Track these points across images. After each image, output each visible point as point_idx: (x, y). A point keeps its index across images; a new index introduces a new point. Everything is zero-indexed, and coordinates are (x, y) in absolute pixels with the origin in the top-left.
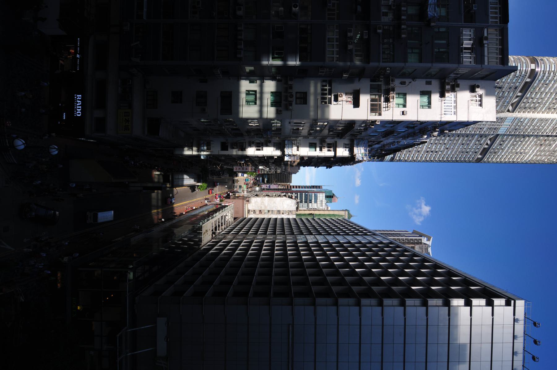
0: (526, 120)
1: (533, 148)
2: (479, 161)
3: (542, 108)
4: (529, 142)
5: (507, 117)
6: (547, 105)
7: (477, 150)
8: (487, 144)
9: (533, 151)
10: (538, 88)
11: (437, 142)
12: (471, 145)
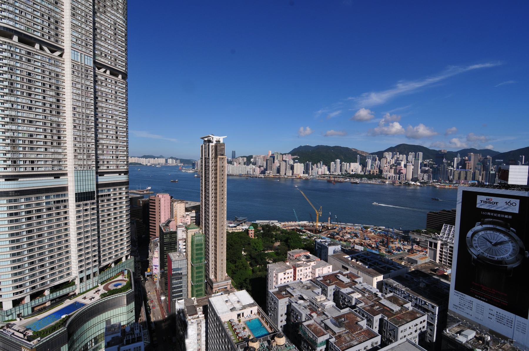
0: (75, 34)
1: (109, 15)
2: (125, 76)
3: (56, 13)
4: (102, 22)
5: (72, 60)
6: (52, 7)
7: (113, 82)
8: (105, 72)
9: (113, 14)
10: (28, 23)
11: (104, 132)
12: (107, 90)
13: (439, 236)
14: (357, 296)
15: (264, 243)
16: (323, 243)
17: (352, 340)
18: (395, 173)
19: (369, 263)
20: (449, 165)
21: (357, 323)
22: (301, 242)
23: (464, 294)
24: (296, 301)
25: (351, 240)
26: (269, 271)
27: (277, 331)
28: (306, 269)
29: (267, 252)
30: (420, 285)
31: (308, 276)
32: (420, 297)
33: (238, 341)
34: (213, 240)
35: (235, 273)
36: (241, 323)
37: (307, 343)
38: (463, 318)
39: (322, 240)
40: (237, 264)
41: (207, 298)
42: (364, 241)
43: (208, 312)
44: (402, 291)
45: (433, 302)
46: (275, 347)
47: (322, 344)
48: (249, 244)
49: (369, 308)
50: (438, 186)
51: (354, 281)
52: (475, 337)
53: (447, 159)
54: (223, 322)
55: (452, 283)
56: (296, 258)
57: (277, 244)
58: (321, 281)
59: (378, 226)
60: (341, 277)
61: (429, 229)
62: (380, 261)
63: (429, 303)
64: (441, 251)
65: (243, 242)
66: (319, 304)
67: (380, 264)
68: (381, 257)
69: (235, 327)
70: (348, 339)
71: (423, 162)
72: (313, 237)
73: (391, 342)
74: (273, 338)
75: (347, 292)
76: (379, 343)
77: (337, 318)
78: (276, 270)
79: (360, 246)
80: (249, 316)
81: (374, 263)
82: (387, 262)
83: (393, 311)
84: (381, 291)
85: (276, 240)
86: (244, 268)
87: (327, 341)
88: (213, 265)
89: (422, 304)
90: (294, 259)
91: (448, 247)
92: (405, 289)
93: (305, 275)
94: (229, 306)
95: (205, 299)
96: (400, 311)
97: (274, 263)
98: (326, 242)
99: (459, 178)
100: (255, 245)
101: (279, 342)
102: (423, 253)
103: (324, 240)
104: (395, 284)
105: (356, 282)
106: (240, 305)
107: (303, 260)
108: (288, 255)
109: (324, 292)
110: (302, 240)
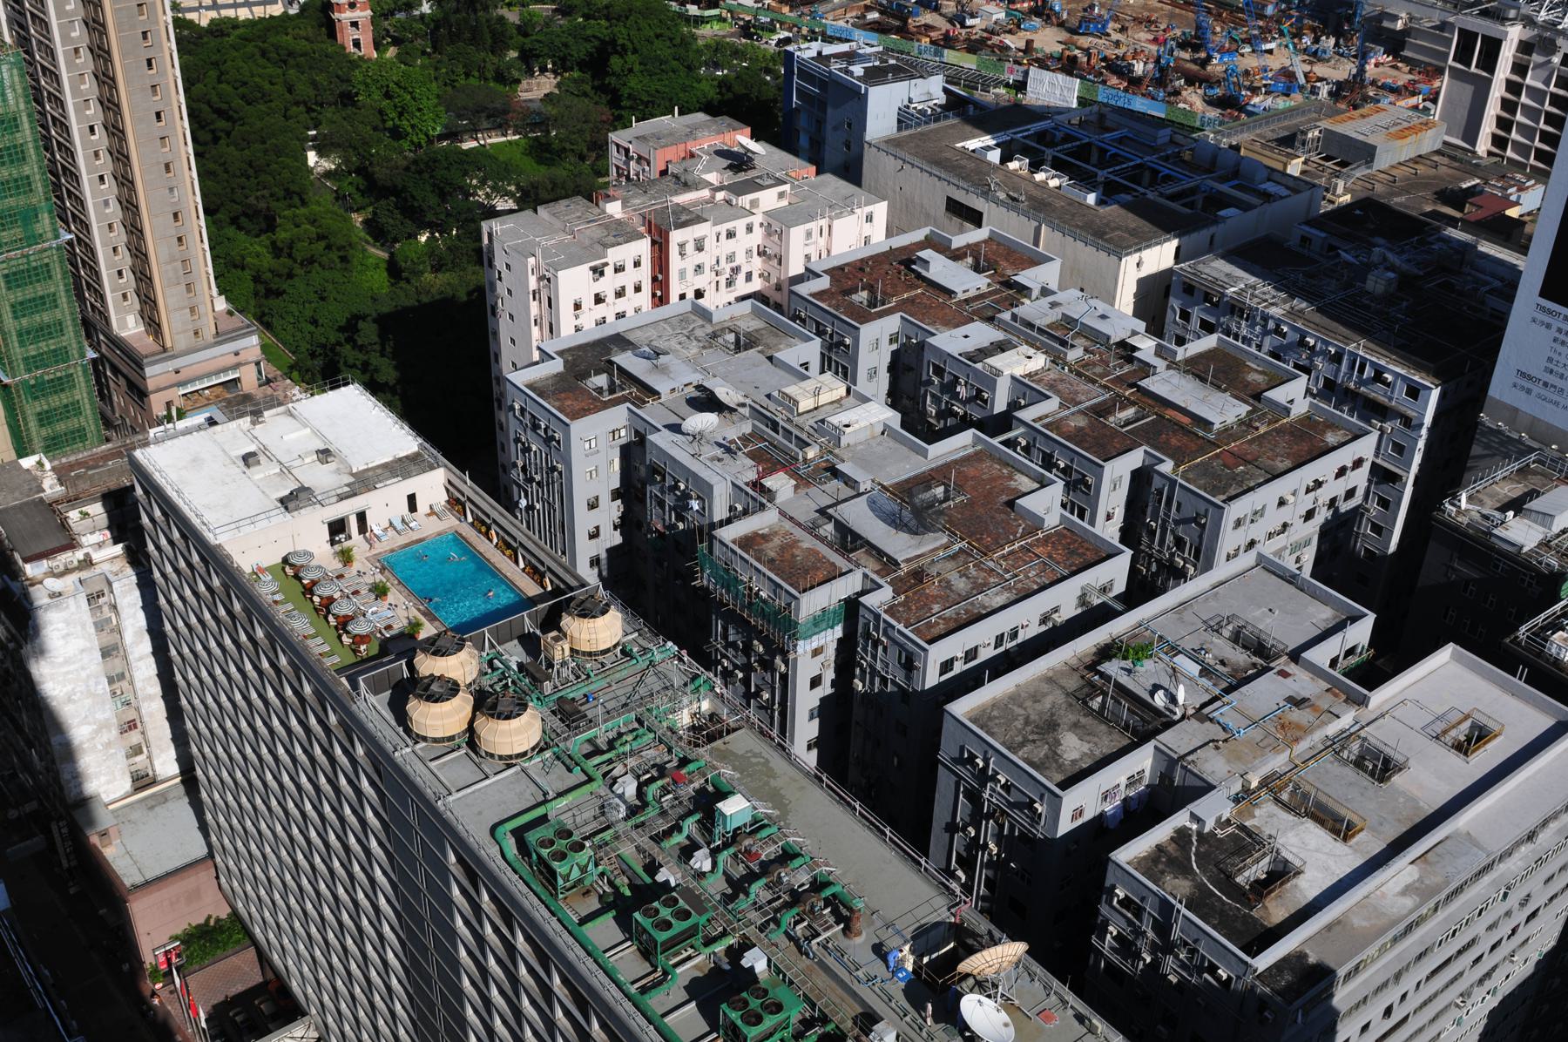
14: (1021, 363)
15: (452, 83)
16: (835, 67)
17: (981, 588)
19: (1102, 175)
21: (1011, 504)
22: (690, 68)
24: (674, 420)
25: (1009, 40)
26: (499, 263)
27: (574, 583)
28: (731, 235)
29: (474, 144)
30: (1370, 284)
31: (741, 277)
32: (1359, 348)
33: (351, 659)
34: (89, 86)
35: (279, 293)
36: (357, 566)
37: (742, 624)
39: (829, 49)
40: (282, 235)
41: (119, 454)
43: (141, 528)
44: (1266, 318)
45: (1419, 368)
46: (564, 664)
47: (821, 621)
48: (348, 99)
49: (1081, 422)
51: (1008, 284)
54: (248, 570)
56: (664, 173)
57: (538, 87)
58: (820, 295)
60: (939, 268)
62: (1166, 159)
63: (1397, 375)
64: (1513, 87)
65: (304, 90)
66: (809, 422)
67: (1167, 178)
68: (1179, 138)
69: (324, 591)
70: (961, 585)
72: (773, 31)
73: (1180, 576)
74: (551, 622)
75: (970, 346)
76: (1120, 587)
77: (906, 490)
78: (539, 252)
79: (1061, 77)
80: (399, 526)
81: (1135, 175)
83: (1207, 424)
84: (1156, 328)
85: (530, 61)
86: (334, 255)
87: (851, 607)
88: (122, 249)
89: (1361, 382)
90: (655, 175)
91: (1556, 60)
92: (1287, 307)
93: (726, 268)
94: (267, 483)
95: (106, 457)
96: (1246, 424)
97: (528, 213)
98: (850, 57)
100: (386, 102)
101: (584, 636)
102: (1413, 101)
103: (844, 47)
104: (1236, 280)
105: (1023, 290)
106: (338, 471)
107: (713, 178)
108: (615, 158)
109: (839, 359)
110: (699, 52)
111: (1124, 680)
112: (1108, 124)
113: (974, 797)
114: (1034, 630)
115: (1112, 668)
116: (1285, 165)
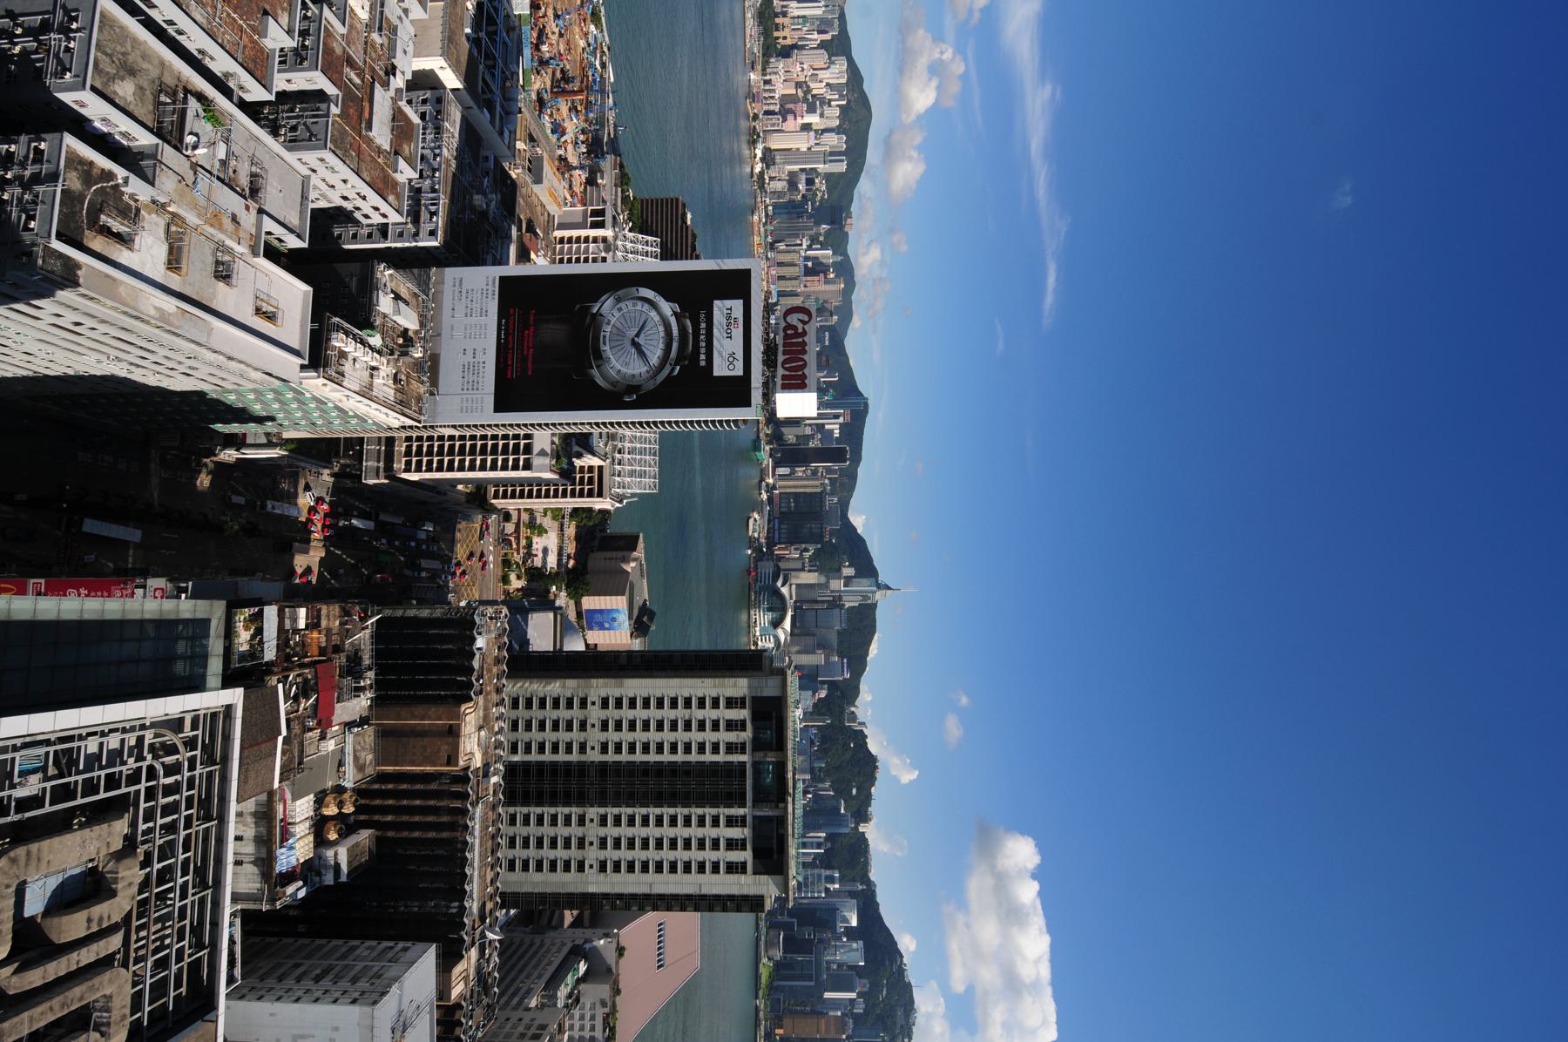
13: (626, 231)
18: (785, 99)
19: (482, 35)
20: (814, 240)
21: (266, 13)
23: (497, 296)
32: (443, 201)
38: (437, 298)
42: (550, 13)
44: (440, 147)
45: (445, 232)
49: (338, 51)
50: (756, 218)
52: (406, 330)
53: (828, 233)
55: (513, 269)
59: (611, 59)
61: (638, 205)
62: (503, 72)
63: (437, 222)
64: (586, 240)
67: (493, 75)
71: (818, 174)
73: (275, 133)
76: (248, 98)
82: (509, 99)
83: (369, 127)
91: (603, 254)
92: (450, 157)
96: (379, 151)
99: (780, 264)
102: (568, 197)
111: (190, 114)
112: (511, 34)
113: (46, 27)
114: (192, 47)
115: (193, 105)
116: (520, 140)
